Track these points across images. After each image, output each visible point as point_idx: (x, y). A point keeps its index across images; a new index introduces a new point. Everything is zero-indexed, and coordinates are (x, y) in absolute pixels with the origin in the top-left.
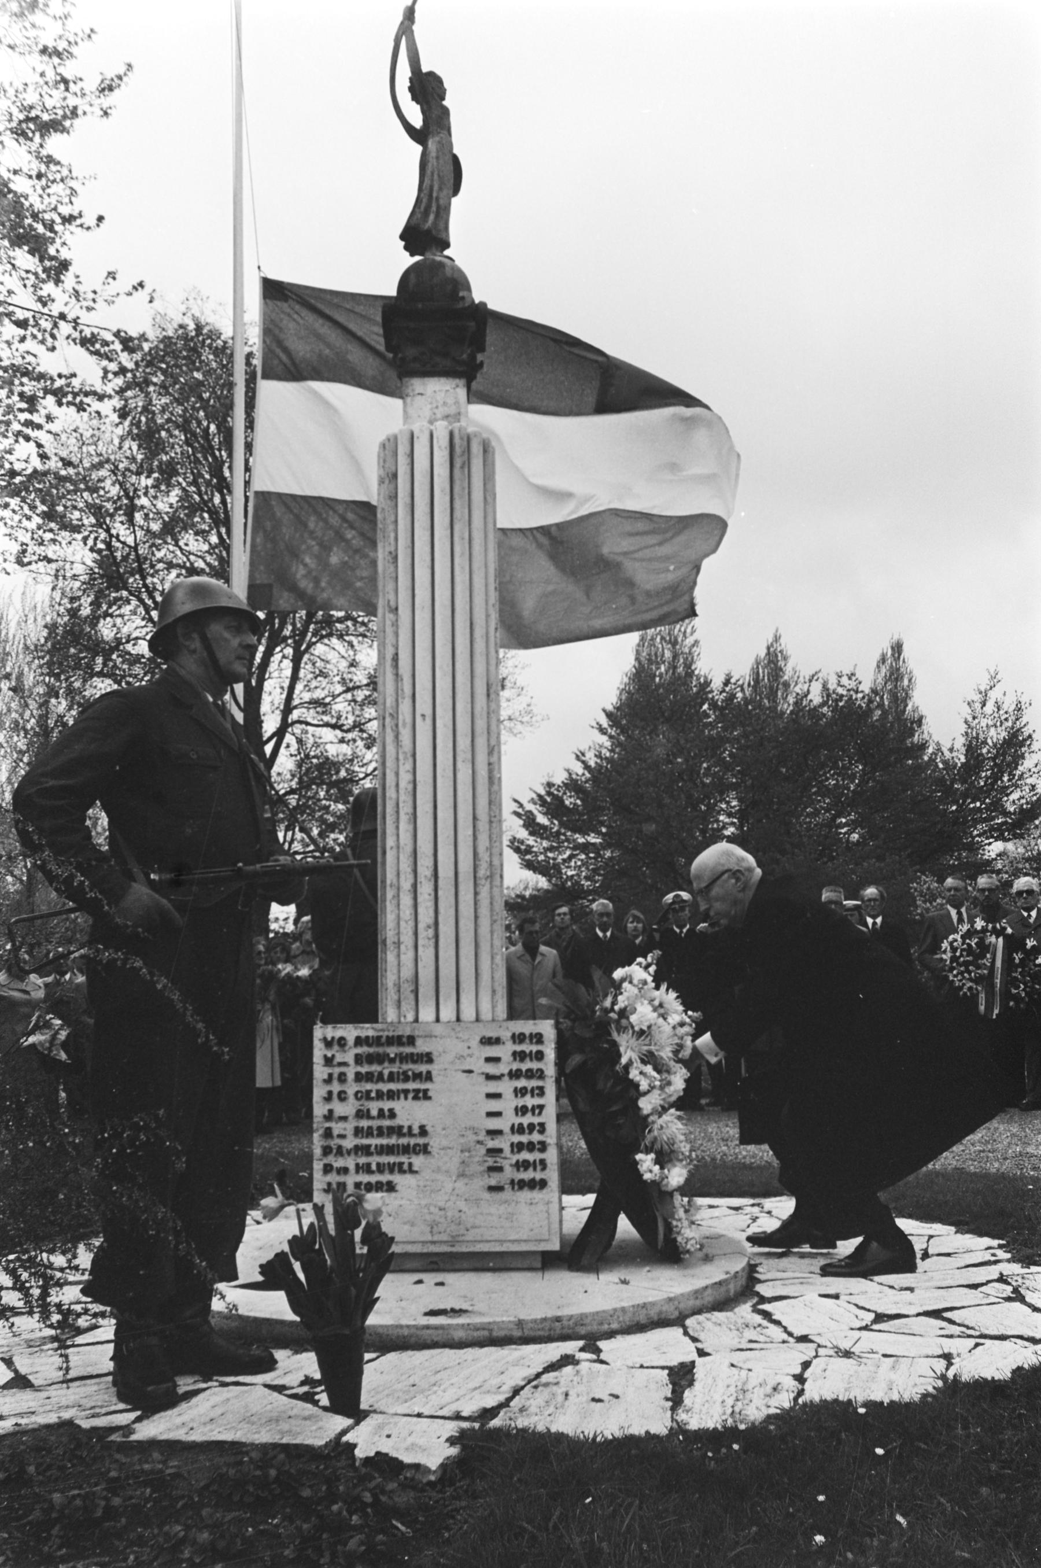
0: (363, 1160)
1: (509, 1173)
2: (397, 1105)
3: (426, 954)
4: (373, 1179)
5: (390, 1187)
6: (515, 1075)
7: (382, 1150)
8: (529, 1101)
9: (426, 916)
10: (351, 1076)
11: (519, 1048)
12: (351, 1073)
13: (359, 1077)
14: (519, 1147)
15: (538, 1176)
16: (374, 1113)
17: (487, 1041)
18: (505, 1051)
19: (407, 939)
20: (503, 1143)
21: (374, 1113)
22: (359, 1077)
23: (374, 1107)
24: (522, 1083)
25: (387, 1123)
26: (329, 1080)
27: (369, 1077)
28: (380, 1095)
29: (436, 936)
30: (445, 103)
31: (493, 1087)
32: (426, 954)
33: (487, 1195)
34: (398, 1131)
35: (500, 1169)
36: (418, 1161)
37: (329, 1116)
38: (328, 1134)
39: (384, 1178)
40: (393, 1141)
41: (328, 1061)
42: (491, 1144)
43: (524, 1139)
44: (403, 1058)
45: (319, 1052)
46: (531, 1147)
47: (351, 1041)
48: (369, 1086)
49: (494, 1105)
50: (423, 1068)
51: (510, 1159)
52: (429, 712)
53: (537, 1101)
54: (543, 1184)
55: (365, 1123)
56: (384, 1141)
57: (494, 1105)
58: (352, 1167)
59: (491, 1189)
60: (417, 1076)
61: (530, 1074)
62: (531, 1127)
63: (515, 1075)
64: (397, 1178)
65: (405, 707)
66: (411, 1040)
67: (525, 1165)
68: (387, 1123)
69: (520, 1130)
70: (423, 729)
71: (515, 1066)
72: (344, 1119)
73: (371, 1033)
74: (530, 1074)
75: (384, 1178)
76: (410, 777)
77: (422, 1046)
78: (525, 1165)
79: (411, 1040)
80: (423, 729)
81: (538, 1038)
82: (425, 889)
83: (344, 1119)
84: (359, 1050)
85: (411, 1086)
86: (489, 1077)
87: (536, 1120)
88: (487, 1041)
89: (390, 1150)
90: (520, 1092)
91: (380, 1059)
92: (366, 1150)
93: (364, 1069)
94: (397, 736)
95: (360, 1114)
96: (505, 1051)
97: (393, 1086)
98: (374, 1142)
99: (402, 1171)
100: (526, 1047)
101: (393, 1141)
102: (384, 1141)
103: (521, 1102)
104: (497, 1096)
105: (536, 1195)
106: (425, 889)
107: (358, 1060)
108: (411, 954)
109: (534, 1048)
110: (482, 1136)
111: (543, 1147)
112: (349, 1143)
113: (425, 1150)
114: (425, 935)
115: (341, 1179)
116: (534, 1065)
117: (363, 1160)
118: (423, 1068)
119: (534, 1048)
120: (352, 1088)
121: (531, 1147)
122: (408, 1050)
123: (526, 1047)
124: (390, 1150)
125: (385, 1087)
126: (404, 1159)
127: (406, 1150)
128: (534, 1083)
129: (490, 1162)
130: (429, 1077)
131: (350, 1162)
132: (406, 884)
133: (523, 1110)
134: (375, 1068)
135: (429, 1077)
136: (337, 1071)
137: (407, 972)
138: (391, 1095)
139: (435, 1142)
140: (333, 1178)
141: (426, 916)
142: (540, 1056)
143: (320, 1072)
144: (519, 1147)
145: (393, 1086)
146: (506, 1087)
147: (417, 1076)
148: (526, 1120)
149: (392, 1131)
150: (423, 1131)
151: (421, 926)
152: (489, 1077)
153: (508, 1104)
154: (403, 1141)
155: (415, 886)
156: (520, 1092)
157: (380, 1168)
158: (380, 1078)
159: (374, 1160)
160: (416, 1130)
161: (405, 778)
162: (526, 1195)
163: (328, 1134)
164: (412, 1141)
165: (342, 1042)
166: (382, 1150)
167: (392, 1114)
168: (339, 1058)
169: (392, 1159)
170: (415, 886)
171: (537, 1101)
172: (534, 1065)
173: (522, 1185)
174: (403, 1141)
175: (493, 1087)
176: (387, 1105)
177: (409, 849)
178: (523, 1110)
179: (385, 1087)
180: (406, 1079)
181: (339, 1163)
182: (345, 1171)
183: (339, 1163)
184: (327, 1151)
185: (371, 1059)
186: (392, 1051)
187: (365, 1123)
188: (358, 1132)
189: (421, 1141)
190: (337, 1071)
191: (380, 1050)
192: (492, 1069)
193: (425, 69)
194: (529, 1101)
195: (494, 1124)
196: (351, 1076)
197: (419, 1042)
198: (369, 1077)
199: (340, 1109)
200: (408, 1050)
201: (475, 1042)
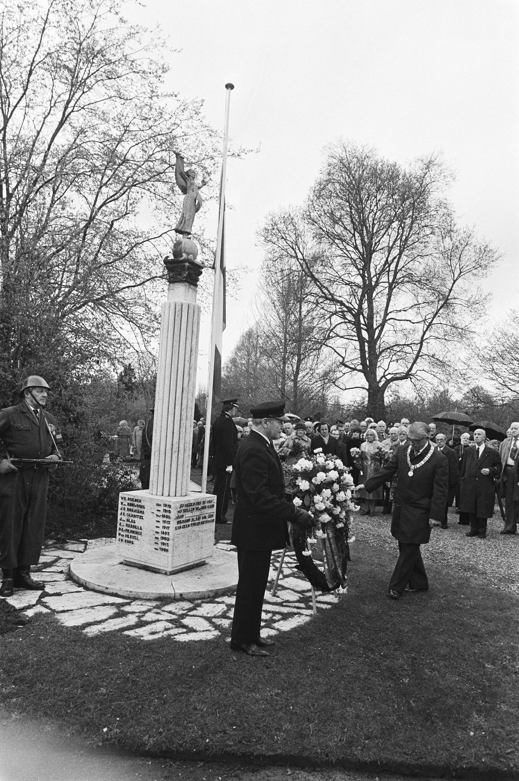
1: (160, 545)
2: (136, 519)
6: (163, 516)
8: (166, 525)
11: (165, 508)
12: (126, 507)
14: (163, 538)
15: (167, 548)
17: (158, 505)
18: (162, 508)
20: (159, 536)
23: (131, 519)
24: (165, 519)
25: (133, 524)
28: (132, 516)
31: (158, 519)
33: (154, 550)
34: (135, 527)
36: (139, 537)
37: (121, 519)
38: (120, 524)
39: (132, 540)
40: (134, 530)
41: (122, 503)
42: (157, 536)
43: (164, 536)
44: (138, 506)
45: (120, 500)
46: (165, 539)
48: (130, 513)
49: (158, 524)
51: (160, 541)
54: (167, 550)
55: (128, 523)
57: (158, 524)
59: (156, 549)
60: (141, 512)
62: (166, 533)
63: (163, 516)
64: (134, 540)
67: (163, 544)
68: (133, 524)
71: (164, 513)
75: (132, 540)
77: (142, 504)
81: (170, 506)
85: (140, 514)
86: (157, 516)
87: (167, 531)
88: (158, 505)
89: (132, 532)
93: (129, 507)
95: (128, 520)
96: (162, 508)
97: (136, 514)
100: (167, 508)
101: (134, 530)
104: (159, 522)
109: (169, 509)
111: (168, 539)
112: (125, 528)
113: (141, 534)
115: (122, 538)
119: (169, 509)
120: (126, 512)
121: (165, 539)
122: (139, 504)
123: (167, 508)
124: (132, 532)
125: (133, 513)
126: (136, 535)
127: (137, 533)
128: (168, 520)
131: (124, 533)
133: (164, 527)
134: (132, 508)
138: (135, 516)
139: (144, 532)
140: (121, 537)
142: (170, 512)
143: (120, 506)
144: (163, 538)
145: (136, 514)
146: (161, 519)
147: (141, 512)
150: (141, 529)
152: (157, 516)
153: (161, 525)
154: (137, 530)
156: (164, 522)
159: (130, 534)
163: (120, 524)
164: (139, 531)
173: (163, 549)
176: (134, 519)
178: (164, 527)
179: (133, 513)
181: (122, 533)
182: (123, 536)
183: (122, 533)
184: (120, 529)
186: (136, 503)
187: (128, 523)
188: (127, 525)
194: (166, 525)
199: (122, 516)
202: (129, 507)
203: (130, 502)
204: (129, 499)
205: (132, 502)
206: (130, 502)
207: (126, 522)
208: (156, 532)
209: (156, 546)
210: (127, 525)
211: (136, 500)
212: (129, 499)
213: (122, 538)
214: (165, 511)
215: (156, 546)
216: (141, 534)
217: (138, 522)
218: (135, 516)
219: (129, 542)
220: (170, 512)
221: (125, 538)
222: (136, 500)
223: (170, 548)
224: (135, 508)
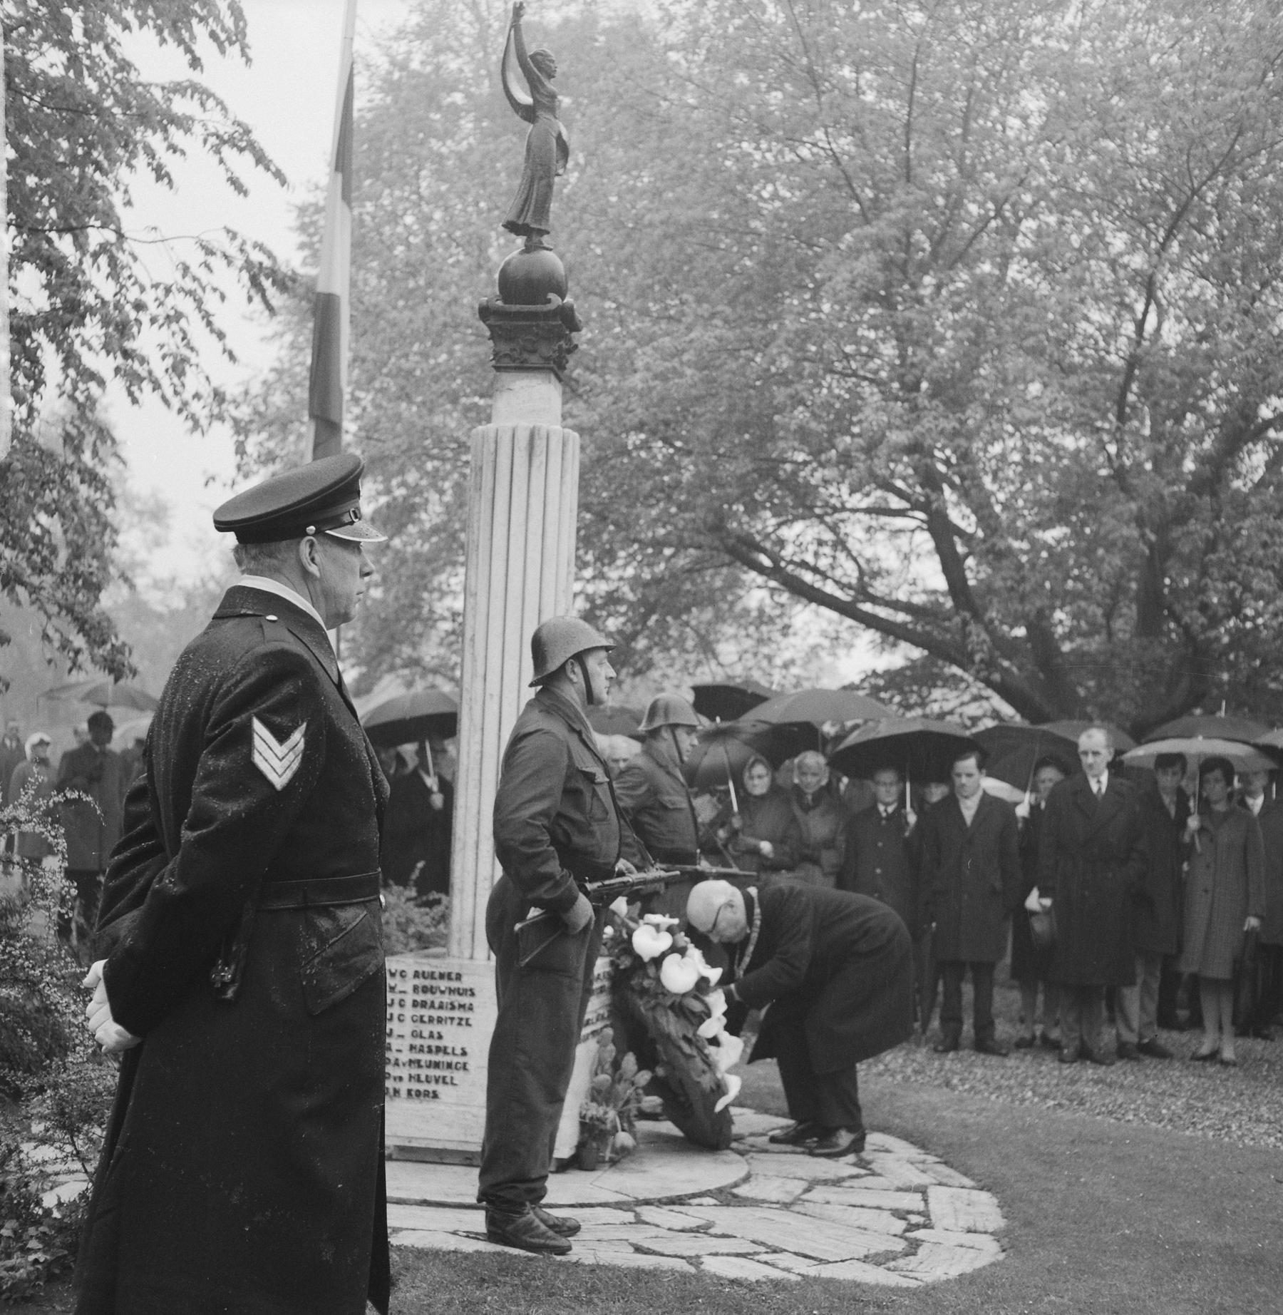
0: (414, 1071)
4: (422, 1087)
10: (409, 1003)
13: (415, 1004)
16: (426, 1034)
21: (426, 1034)
22: (415, 1004)
23: (426, 1029)
25: (434, 1043)
27: (424, 1004)
28: (431, 1020)
36: (458, 1076)
39: (431, 1087)
40: (439, 1058)
44: (451, 991)
47: (410, 974)
50: (465, 1000)
52: (496, 692)
55: (418, 1042)
58: (406, 1077)
60: (462, 1006)
64: (440, 1088)
72: (401, 1036)
73: (427, 969)
76: (477, 748)
77: (466, 983)
79: (459, 977)
83: (401, 1036)
85: (457, 1014)
92: (418, 1063)
93: (420, 997)
98: (425, 1057)
99: (445, 1082)
101: (439, 1058)
107: (415, 989)
108: (471, 900)
112: (405, 1056)
117: (414, 1071)
118: (465, 1000)
120: (409, 1012)
122: (454, 985)
125: (435, 1013)
126: (447, 1073)
130: (471, 1008)
134: (428, 997)
135: (471, 1008)
138: (440, 1020)
147: (462, 1006)
150: (464, 1053)
151: (480, 878)
157: (428, 1080)
158: (432, 1006)
159: (424, 1072)
160: (458, 1051)
161: (476, 748)
164: (454, 1060)
167: (440, 1037)
168: (399, 988)
169: (438, 1073)
176: (436, 1028)
177: (474, 811)
179: (435, 1013)
180: (453, 1008)
182: (401, 1079)
185: (425, 990)
186: (443, 984)
187: (418, 1042)
188: (412, 1048)
189: (462, 1060)
191: (434, 983)
193: (531, 49)
196: (409, 1003)
197: (464, 978)
198: (424, 1004)
200: (454, 985)
202: (420, 997)
203: (420, 982)
204: (416, 975)
205: (428, 983)
206: (420, 982)
207: (409, 1040)
210: (412, 1048)
211: (442, 976)
216: (465, 1067)
218: (440, 1020)
221: (404, 1087)
222: (442, 976)
224: (438, 998)
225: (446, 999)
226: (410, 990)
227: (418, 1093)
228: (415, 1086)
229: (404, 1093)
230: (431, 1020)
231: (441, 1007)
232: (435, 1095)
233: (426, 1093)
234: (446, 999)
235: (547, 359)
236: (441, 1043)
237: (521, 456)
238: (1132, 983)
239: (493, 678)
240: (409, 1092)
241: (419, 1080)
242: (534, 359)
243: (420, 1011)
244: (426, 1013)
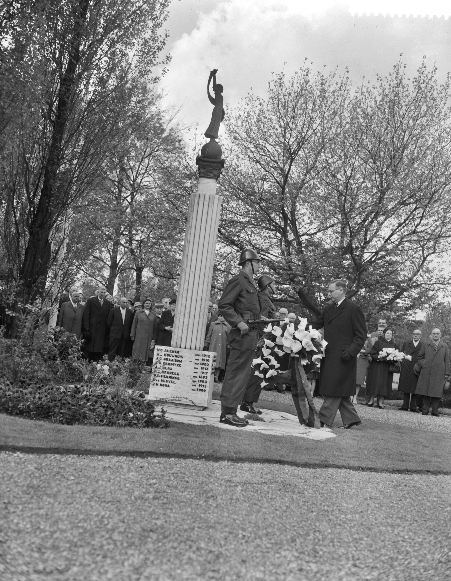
1: (197, 387)
3: (185, 332)
4: (165, 383)
5: (169, 386)
7: (167, 377)
8: (204, 371)
9: (186, 323)
11: (204, 358)
12: (163, 357)
13: (164, 359)
14: (201, 381)
15: (204, 388)
17: (197, 355)
19: (181, 328)
22: (164, 359)
23: (167, 366)
24: (203, 366)
25: (169, 371)
26: (157, 359)
27: (167, 359)
28: (169, 364)
29: (188, 328)
30: (222, 94)
31: (196, 366)
32: (185, 332)
34: (172, 373)
35: (195, 386)
36: (176, 381)
38: (155, 371)
39: (168, 384)
40: (171, 375)
41: (158, 354)
42: (195, 379)
43: (202, 379)
44: (176, 356)
46: (203, 382)
49: (196, 370)
51: (197, 384)
53: (206, 371)
54: (205, 390)
56: (169, 375)
57: (196, 370)
60: (178, 361)
61: (205, 364)
62: (204, 377)
63: (202, 364)
64: (170, 384)
65: (188, 269)
66: (178, 352)
67: (201, 386)
69: (201, 377)
70: (192, 275)
71: (202, 362)
74: (205, 364)
77: (180, 354)
78: (201, 386)
79: (178, 352)
80: (192, 275)
82: (187, 316)
84: (166, 353)
85: (177, 363)
86: (195, 364)
87: (205, 375)
88: (197, 355)
89: (170, 377)
90: (203, 368)
91: (170, 356)
93: (166, 357)
94: (185, 275)
96: (200, 358)
97: (172, 362)
100: (206, 358)
101: (171, 375)
102: (169, 375)
103: (202, 371)
105: (203, 392)
106: (187, 316)
107: (165, 355)
108: (181, 331)
110: (192, 377)
111: (206, 382)
113: (178, 379)
114: (185, 327)
115: (157, 382)
116: (207, 362)
117: (163, 379)
119: (207, 358)
121: (203, 382)
122: (177, 354)
124: (170, 377)
125: (170, 362)
126: (172, 380)
127: (173, 378)
129: (193, 384)
130: (181, 361)
131: (160, 379)
132: (182, 314)
134: (169, 358)
135: (181, 361)
136: (159, 357)
137: (180, 336)
138: (172, 364)
141: (186, 323)
145: (172, 362)
146: (199, 366)
147: (178, 361)
148: (203, 375)
149: (170, 373)
150: (178, 374)
152: (195, 364)
153: (199, 371)
154: (173, 376)
155: (184, 315)
156: (203, 368)
158: (170, 360)
159: (165, 379)
161: (186, 287)
162: (201, 392)
164: (175, 376)
165: (161, 350)
166: (167, 377)
169: (170, 379)
170: (184, 315)
171: (206, 371)
172: (207, 362)
173: (200, 390)
174: (173, 376)
175: (196, 366)
176: (170, 366)
177: (184, 305)
179: (170, 362)
185: (168, 355)
186: (173, 354)
189: (177, 376)
190: (159, 357)
192: (197, 362)
193: (218, 83)
194: (204, 371)
195: (195, 375)
196: (163, 359)
198: (167, 359)
200: (177, 354)
201: (193, 355)
202: (166, 357)
203: (167, 353)
205: (169, 353)
206: (167, 353)
208: (194, 377)
209: (194, 388)
211: (173, 352)
212: (165, 351)
213: (157, 382)
214: (204, 360)
215: (194, 388)
217: (175, 369)
218: (172, 364)
219: (166, 385)
220: (208, 360)
221: (159, 383)
222: (173, 352)
223: (207, 389)
224: (171, 358)
225: (174, 358)
226: (163, 355)
227: (164, 385)
228: (163, 383)
229: (159, 385)
230: (169, 364)
231: (172, 360)
232: (169, 386)
233: (166, 385)
234: (174, 358)
235: (215, 175)
236: (171, 371)
237: (206, 203)
238: (354, 394)
239: (193, 267)
240: (161, 385)
241: (164, 381)
242: (212, 175)
243: (166, 361)
244: (168, 362)
